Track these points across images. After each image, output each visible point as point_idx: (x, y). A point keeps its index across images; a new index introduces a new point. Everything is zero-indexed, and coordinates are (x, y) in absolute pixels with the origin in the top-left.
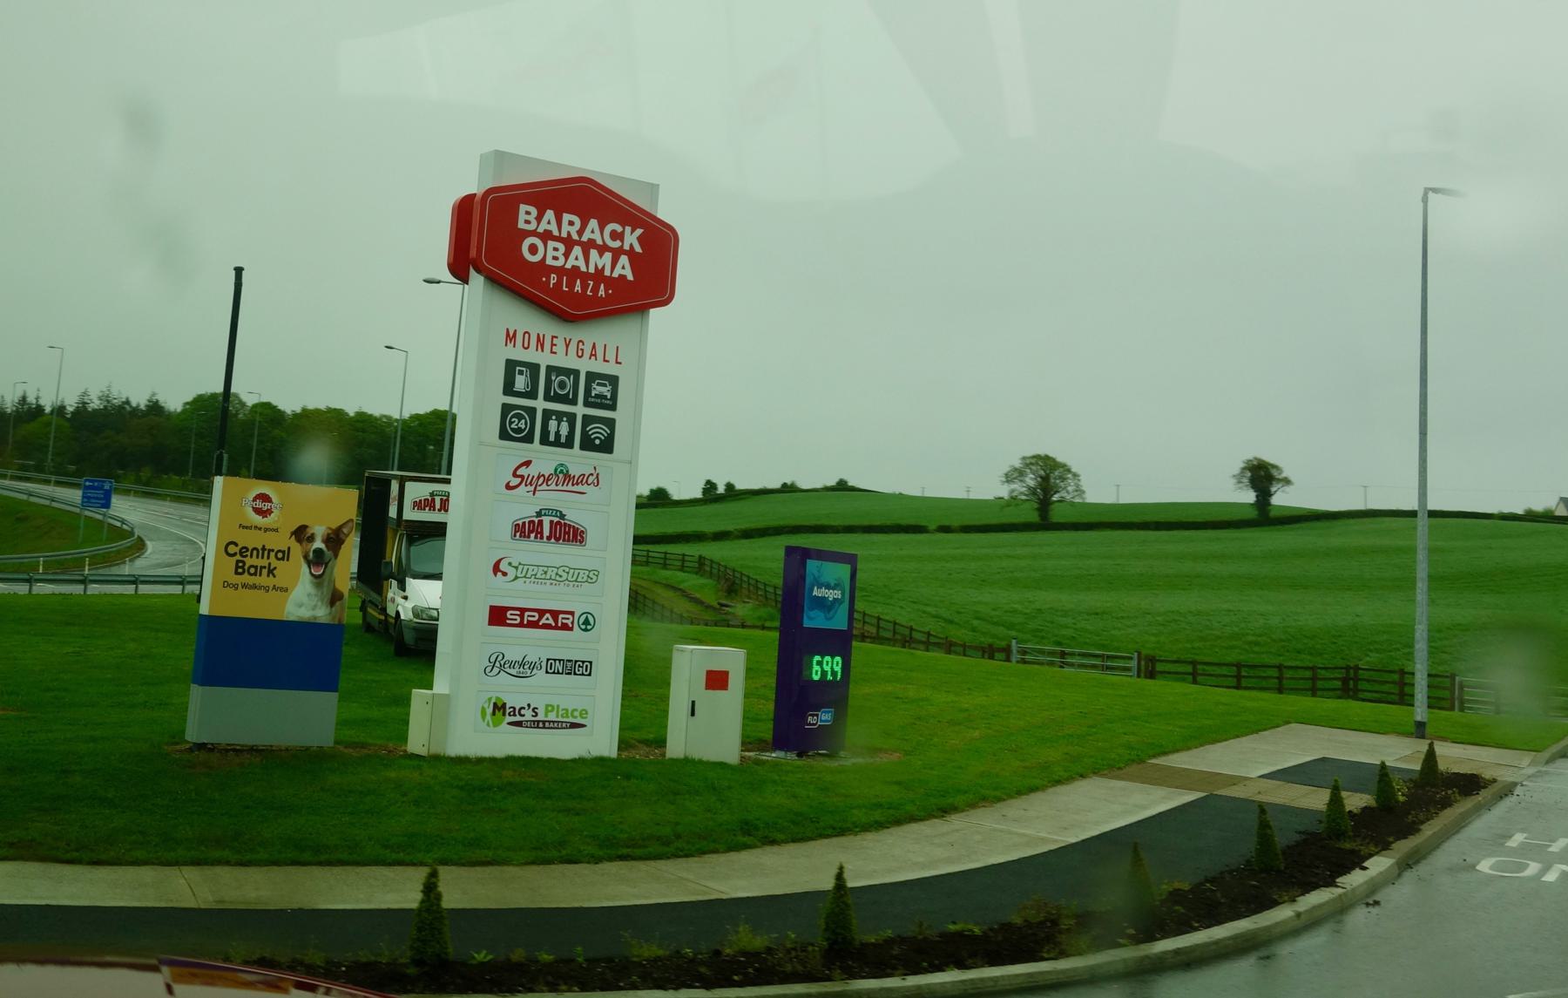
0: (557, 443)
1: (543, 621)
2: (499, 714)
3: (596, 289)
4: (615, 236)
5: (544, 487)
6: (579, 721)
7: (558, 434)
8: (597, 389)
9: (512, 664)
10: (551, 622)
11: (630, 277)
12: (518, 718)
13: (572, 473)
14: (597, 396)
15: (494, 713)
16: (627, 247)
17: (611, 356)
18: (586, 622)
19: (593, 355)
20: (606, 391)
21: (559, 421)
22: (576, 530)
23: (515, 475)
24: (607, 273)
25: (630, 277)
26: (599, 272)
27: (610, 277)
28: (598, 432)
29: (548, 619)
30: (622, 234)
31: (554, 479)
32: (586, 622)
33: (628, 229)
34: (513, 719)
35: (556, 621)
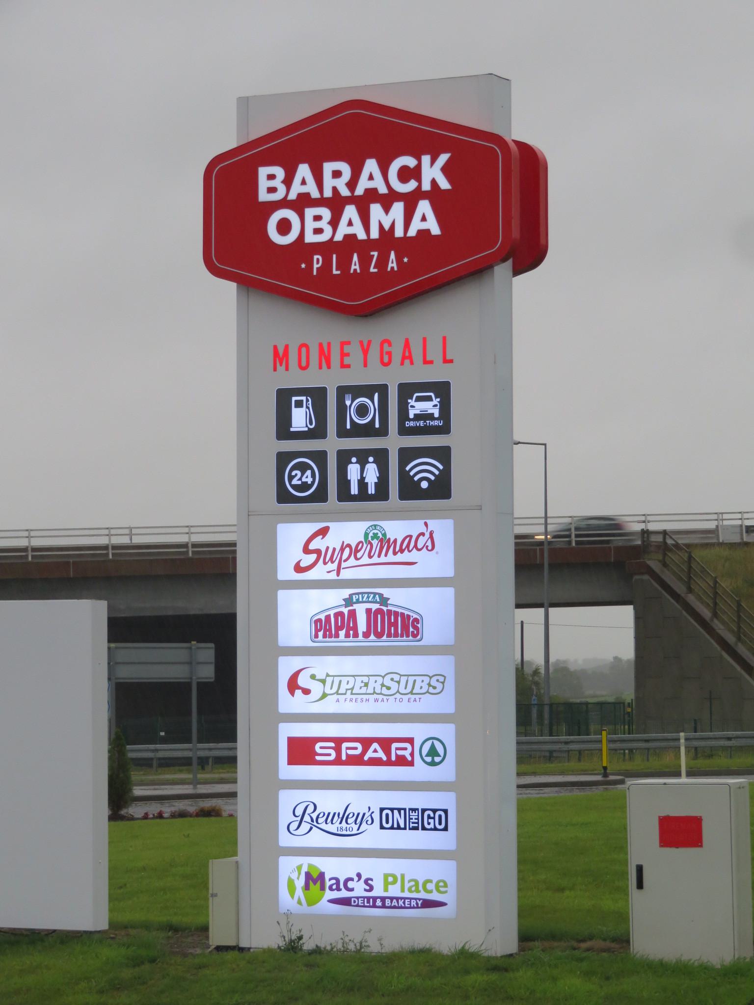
0: (363, 495)
1: (370, 754)
2: (315, 888)
3: (383, 261)
4: (405, 174)
5: (352, 561)
6: (435, 896)
7: (362, 484)
8: (417, 407)
9: (329, 818)
10: (381, 754)
11: (436, 230)
12: (344, 894)
13: (391, 536)
14: (418, 417)
15: (307, 887)
16: (426, 186)
17: (435, 353)
18: (433, 752)
19: (407, 357)
20: (431, 407)
21: (363, 463)
22: (405, 618)
23: (306, 550)
24: (399, 233)
25: (436, 230)
26: (387, 234)
27: (405, 238)
28: (424, 470)
29: (375, 752)
30: (418, 167)
31: (366, 548)
32: (433, 752)
33: (426, 159)
34: (336, 895)
35: (388, 752)
